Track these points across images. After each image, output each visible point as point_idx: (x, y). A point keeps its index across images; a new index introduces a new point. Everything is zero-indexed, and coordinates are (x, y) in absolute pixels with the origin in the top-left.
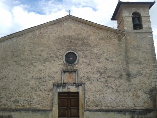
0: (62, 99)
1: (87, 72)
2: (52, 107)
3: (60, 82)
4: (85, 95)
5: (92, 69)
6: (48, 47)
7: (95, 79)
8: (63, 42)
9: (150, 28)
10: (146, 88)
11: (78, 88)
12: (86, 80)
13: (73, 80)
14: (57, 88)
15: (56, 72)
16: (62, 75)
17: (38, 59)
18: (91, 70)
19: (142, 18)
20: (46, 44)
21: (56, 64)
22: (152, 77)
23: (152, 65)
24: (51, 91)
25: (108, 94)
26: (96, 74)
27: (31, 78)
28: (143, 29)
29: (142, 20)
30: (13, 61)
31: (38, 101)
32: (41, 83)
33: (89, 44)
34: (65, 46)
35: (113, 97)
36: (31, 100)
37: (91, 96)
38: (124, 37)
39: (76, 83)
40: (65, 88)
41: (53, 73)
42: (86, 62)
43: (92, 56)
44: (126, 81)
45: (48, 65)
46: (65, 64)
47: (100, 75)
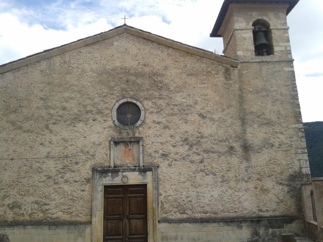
1: (161, 143)
2: (91, 215)
3: (107, 164)
4: (158, 189)
5: (171, 136)
6: (81, 90)
7: (180, 157)
8: (113, 82)
9: (289, 52)
10: (282, 173)
11: (144, 176)
13: (134, 159)
14: (101, 177)
15: (97, 143)
17: (61, 116)
18: (170, 139)
19: (272, 31)
21: (98, 127)
22: (293, 152)
23: (294, 126)
24: (88, 183)
26: (181, 147)
27: (47, 157)
29: (273, 35)
30: (7, 122)
31: (63, 204)
32: (67, 166)
33: (167, 85)
34: (115, 88)
35: (216, 193)
36: (47, 201)
38: (236, 72)
39: (139, 166)
40: (118, 176)
41: (92, 145)
44: (241, 160)
45: (81, 130)
46: (116, 126)
47: (189, 149)
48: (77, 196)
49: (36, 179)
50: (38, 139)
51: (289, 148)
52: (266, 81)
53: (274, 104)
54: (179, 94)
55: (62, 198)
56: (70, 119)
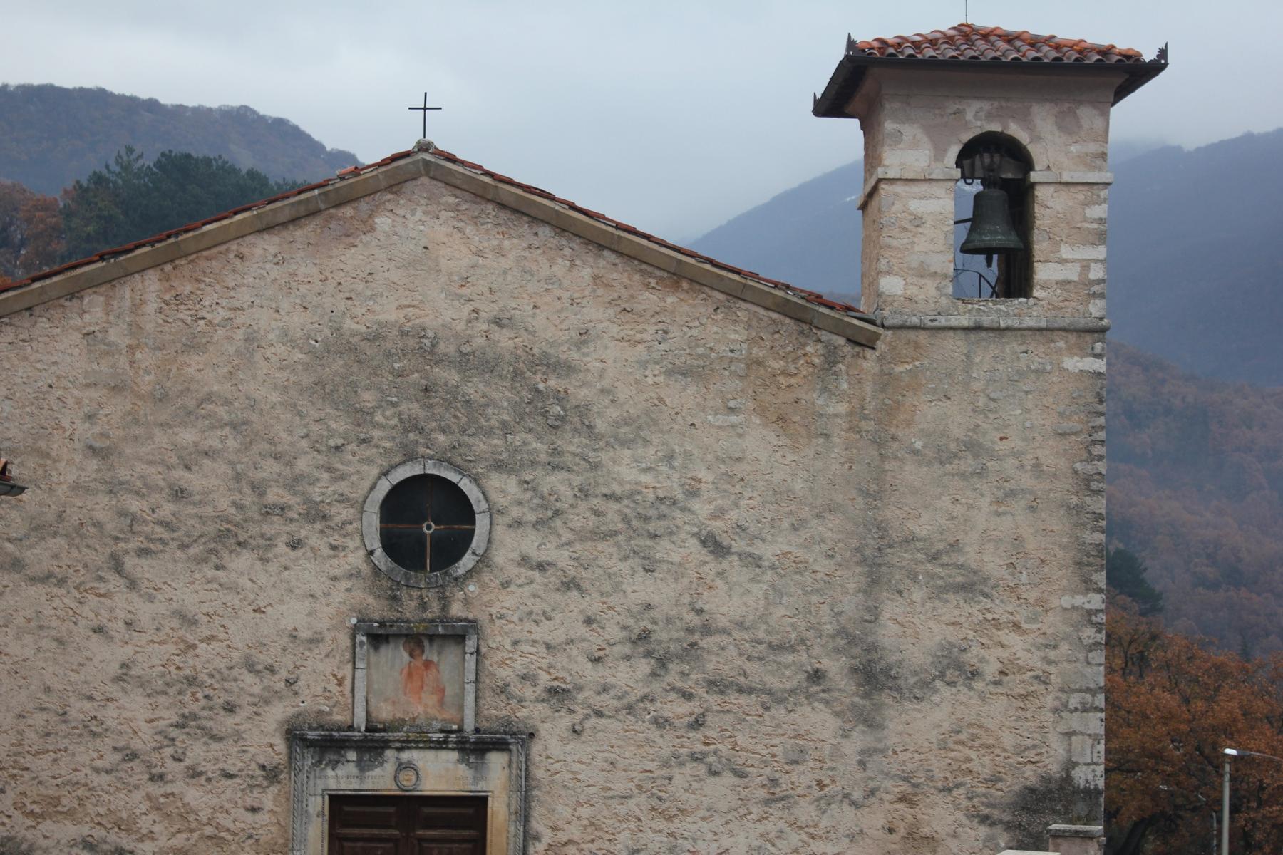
0: (359, 844)
1: (548, 647)
3: (339, 717)
4: (526, 819)
5: (589, 621)
6: (245, 423)
7: (616, 703)
10: (995, 779)
12: (540, 706)
13: (441, 702)
14: (320, 762)
16: (359, 665)
17: (167, 525)
18: (582, 631)
19: (1040, 192)
20: (227, 402)
21: (308, 572)
22: (1050, 701)
23: (1066, 601)
24: (271, 783)
25: (703, 819)
26: (623, 665)
27: (119, 679)
28: (1035, 293)
29: (1037, 209)
32: (195, 717)
33: (583, 410)
34: (379, 418)
37: (574, 832)
39: (460, 730)
40: (382, 764)
41: (286, 640)
42: (549, 564)
43: (597, 513)
44: (849, 726)
45: (244, 582)
46: (376, 570)
47: (654, 674)
48: (231, 827)
49: (85, 759)
50: (86, 611)
51: (1035, 687)
52: (985, 412)
53: (1001, 510)
54: (627, 452)
55: (179, 831)
56: (201, 536)
